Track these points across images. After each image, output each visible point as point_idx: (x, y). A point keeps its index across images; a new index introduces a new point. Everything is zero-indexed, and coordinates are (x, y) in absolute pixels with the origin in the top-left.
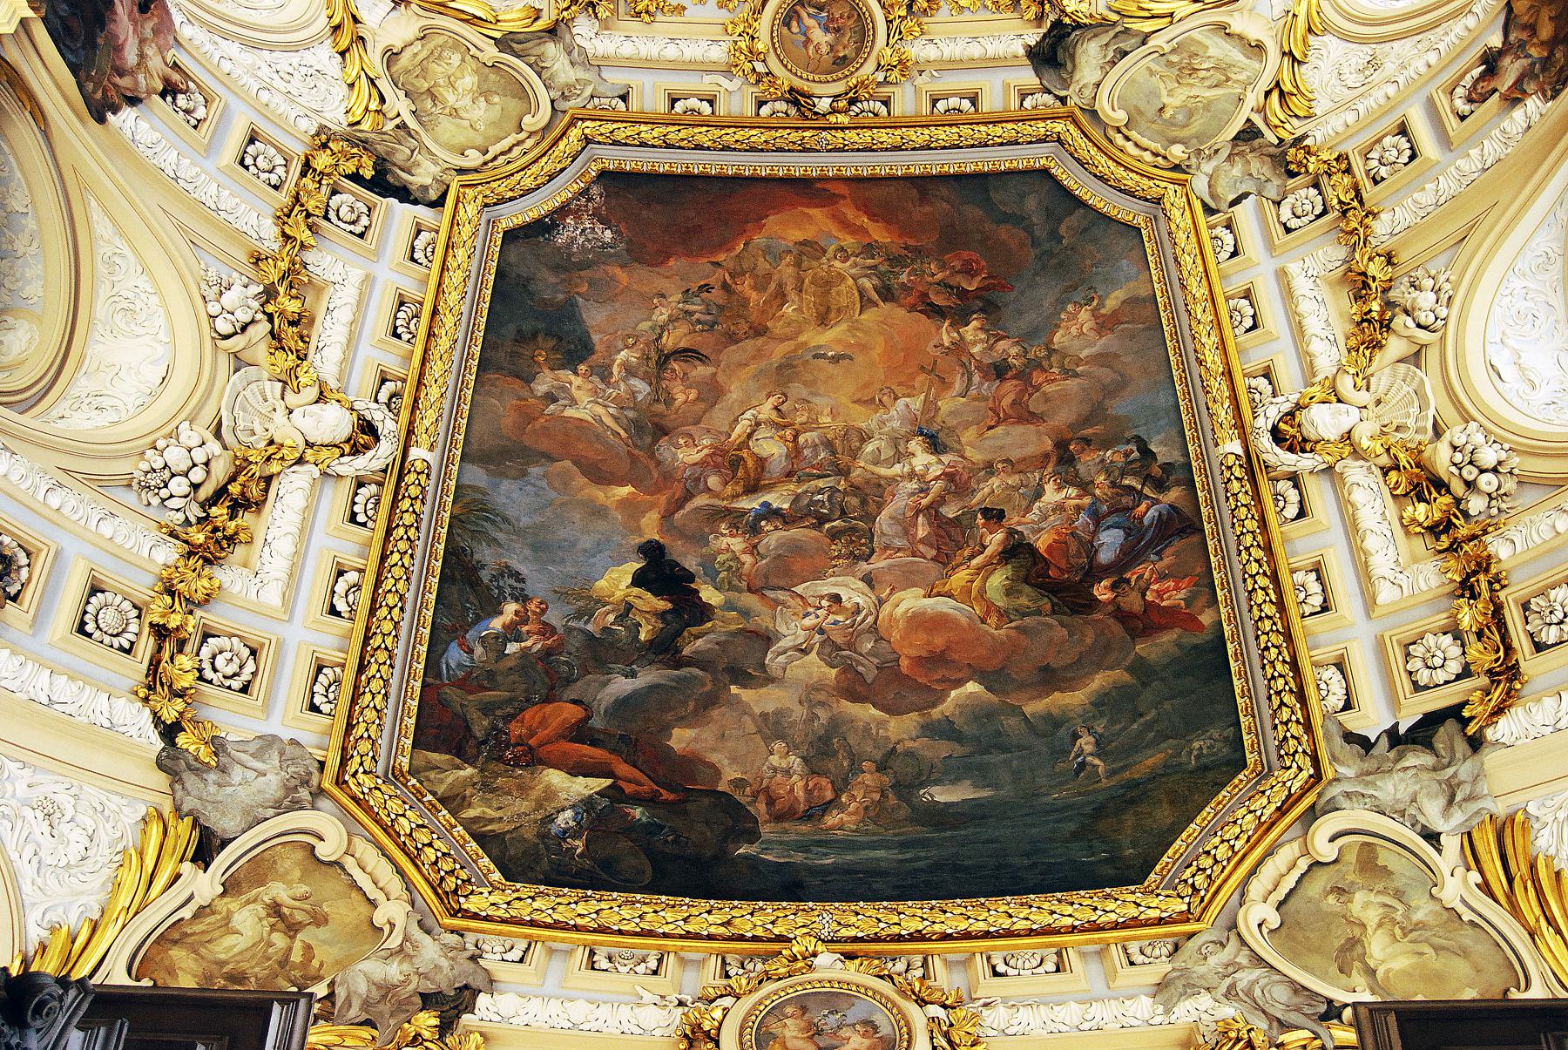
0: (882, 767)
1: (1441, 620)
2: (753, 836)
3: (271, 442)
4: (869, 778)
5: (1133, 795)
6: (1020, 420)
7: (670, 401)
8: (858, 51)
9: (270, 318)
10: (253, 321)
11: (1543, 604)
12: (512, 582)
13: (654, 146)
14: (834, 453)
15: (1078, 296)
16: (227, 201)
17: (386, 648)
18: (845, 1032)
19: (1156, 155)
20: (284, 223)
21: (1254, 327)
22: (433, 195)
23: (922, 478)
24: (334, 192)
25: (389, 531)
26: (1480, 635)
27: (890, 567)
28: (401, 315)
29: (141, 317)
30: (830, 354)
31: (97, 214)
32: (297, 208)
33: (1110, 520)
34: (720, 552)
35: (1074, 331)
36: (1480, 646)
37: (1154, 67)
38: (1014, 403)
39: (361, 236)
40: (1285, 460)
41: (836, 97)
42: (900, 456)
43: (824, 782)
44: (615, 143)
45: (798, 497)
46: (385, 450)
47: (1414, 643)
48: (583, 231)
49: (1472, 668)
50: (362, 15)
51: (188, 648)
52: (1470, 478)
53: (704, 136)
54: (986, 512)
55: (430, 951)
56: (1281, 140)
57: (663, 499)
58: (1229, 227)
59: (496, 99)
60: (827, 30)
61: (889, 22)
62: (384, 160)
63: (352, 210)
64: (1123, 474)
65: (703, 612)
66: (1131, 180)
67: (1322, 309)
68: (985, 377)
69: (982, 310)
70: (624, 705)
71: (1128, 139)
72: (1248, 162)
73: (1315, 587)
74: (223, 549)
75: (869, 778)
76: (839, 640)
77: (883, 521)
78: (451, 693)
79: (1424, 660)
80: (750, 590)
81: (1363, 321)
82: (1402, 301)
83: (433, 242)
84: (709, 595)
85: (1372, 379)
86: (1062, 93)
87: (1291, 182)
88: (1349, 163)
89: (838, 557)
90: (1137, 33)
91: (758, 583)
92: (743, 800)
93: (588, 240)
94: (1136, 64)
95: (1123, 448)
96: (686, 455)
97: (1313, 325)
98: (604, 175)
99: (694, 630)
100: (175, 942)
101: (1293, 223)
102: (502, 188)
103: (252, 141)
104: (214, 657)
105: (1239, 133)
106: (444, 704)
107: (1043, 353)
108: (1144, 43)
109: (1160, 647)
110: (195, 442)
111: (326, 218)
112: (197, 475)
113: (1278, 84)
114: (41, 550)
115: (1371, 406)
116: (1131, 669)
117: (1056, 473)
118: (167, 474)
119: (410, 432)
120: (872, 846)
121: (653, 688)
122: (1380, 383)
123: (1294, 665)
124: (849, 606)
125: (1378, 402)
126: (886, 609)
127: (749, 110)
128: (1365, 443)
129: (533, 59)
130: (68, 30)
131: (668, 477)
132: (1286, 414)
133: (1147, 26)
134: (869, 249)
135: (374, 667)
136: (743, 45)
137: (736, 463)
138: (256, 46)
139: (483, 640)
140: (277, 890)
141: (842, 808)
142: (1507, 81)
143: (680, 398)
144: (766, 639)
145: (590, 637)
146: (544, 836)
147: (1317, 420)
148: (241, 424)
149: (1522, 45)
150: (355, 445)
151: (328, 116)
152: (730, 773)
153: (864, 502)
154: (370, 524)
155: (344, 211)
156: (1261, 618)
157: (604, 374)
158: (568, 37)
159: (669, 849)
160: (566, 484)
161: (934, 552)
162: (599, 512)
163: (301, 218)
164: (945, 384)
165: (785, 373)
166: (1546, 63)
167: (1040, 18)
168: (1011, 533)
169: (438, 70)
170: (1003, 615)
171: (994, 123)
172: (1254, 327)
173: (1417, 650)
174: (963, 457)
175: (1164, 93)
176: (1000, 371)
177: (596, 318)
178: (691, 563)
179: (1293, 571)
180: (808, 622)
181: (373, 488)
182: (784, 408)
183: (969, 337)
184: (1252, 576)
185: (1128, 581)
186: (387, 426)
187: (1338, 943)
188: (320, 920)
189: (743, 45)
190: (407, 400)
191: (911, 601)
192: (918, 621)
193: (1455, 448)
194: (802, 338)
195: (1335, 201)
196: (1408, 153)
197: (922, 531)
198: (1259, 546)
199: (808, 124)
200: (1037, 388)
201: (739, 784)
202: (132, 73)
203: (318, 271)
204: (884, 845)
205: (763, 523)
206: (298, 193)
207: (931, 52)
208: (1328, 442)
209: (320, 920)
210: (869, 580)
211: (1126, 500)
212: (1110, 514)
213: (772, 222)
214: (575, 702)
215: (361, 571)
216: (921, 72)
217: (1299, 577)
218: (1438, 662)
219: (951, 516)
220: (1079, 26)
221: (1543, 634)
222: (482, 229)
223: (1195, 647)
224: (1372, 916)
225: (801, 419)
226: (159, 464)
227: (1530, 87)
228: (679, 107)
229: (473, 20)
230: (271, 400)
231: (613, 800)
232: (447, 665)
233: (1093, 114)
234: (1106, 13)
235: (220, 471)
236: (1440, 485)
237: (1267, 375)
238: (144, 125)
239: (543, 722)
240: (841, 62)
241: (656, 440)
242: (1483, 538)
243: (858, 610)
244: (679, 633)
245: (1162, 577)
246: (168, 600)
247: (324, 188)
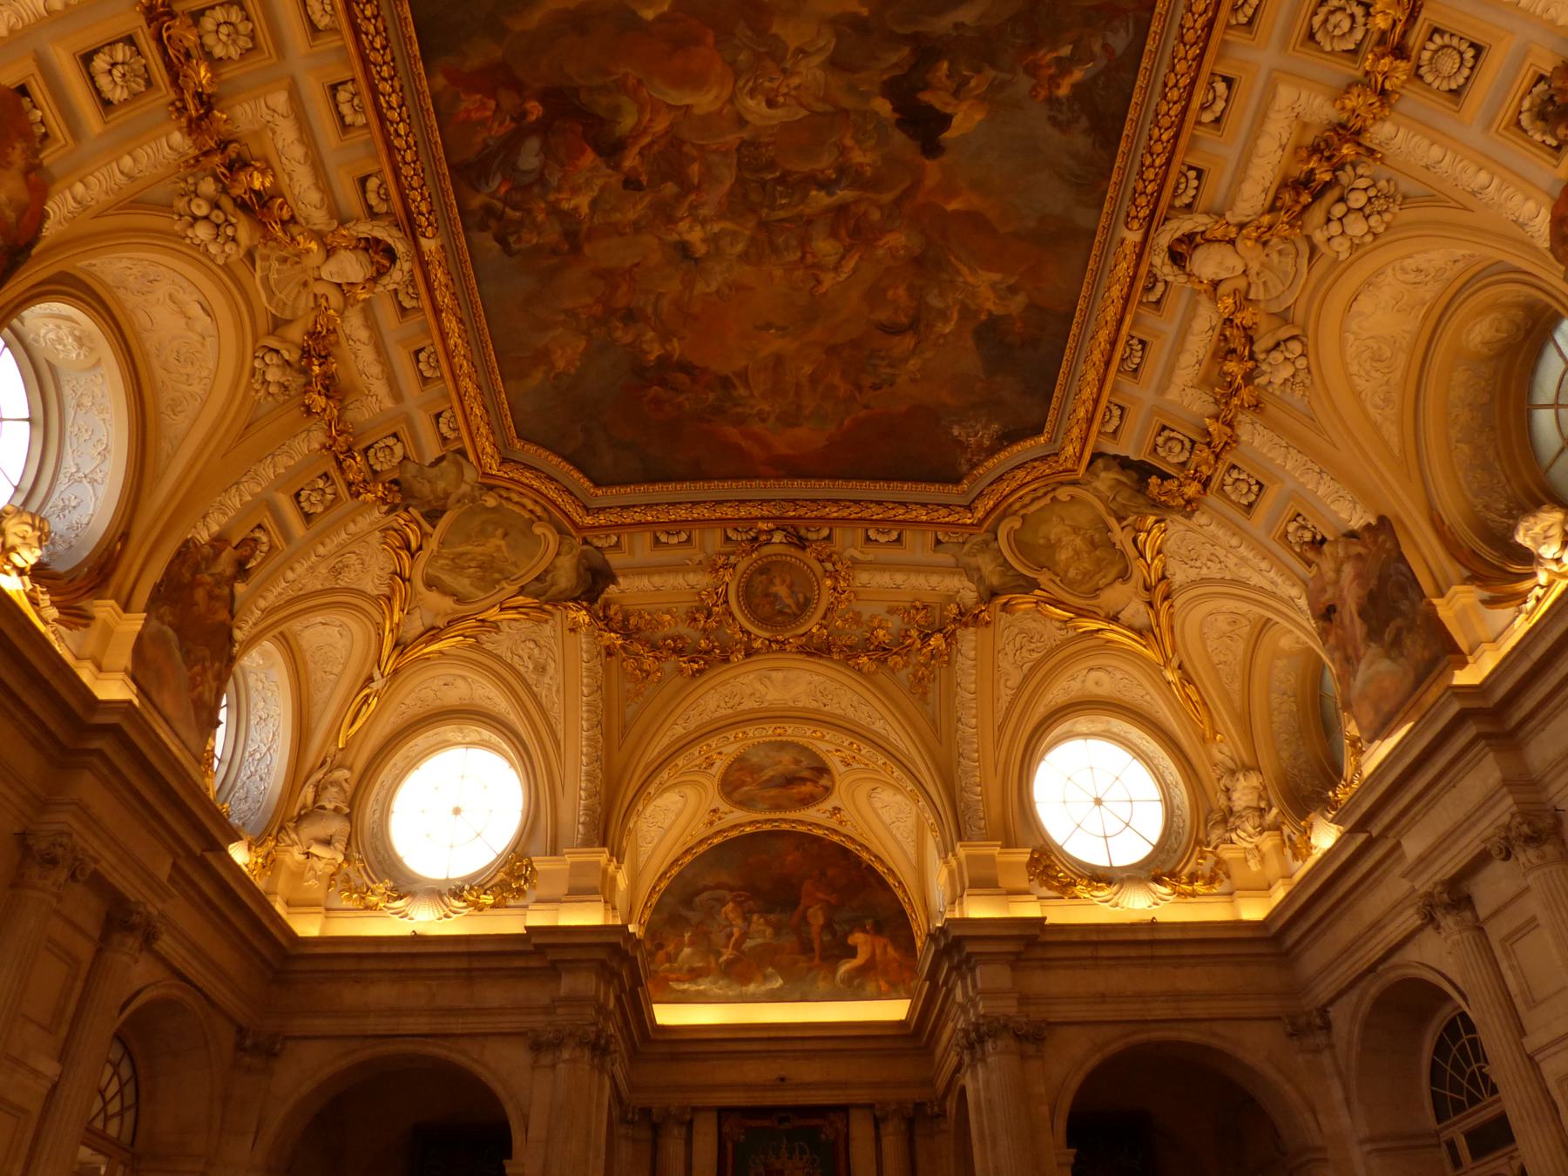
1: (228, 72)
3: (1265, 244)
8: (750, 580)
9: (1252, 356)
10: (1268, 352)
11: (134, 85)
12: (1061, 117)
13: (916, 504)
16: (1277, 456)
17: (1185, 45)
19: (508, 499)
20: (1231, 437)
21: (417, 353)
22: (1100, 463)
24: (1184, 464)
25: (1168, 162)
26: (188, 55)
28: (1137, 360)
29: (1367, 355)
30: (773, 331)
31: (1394, 441)
32: (1218, 450)
35: (569, 351)
36: (186, 44)
37: (513, 569)
39: (1164, 428)
40: (381, 232)
41: (768, 542)
42: (713, 240)
44: (947, 506)
45: (804, 199)
46: (1164, 238)
47: (248, 50)
48: (976, 435)
49: (190, 21)
50: (1143, 608)
51: (1375, 37)
52: (216, 212)
53: (876, 512)
54: (638, 187)
56: (406, 510)
58: (444, 439)
59: (1041, 541)
60: (776, 596)
61: (726, 602)
62: (1139, 491)
63: (1170, 450)
64: (521, 223)
66: (527, 477)
67: (361, 367)
71: (531, 512)
72: (433, 492)
73: (345, 109)
74: (1326, 141)
77: (728, 178)
79: (237, 32)
80: (846, 112)
81: (325, 357)
82: (294, 373)
83: (1104, 423)
84: (883, 107)
85: (312, 305)
86: (585, 547)
87: (396, 475)
88: (349, 490)
89: (768, 144)
90: (526, 596)
93: (972, 426)
94: (528, 571)
95: (523, 246)
96: (898, 240)
97: (367, 355)
98: (957, 481)
99: (898, 72)
101: (391, 441)
102: (1043, 468)
103: (1250, 505)
104: (1352, 29)
105: (441, 516)
107: (594, 331)
108: (522, 588)
109: (480, 54)
110: (1335, 242)
111: (1193, 442)
112: (1339, 210)
113: (412, 556)
114: (1506, 128)
115: (311, 280)
118: (1367, 211)
119: (1140, 256)
122: (306, 302)
123: (356, 31)
124: (760, 97)
125: (305, 284)
126: (726, 93)
127: (837, 532)
128: (314, 246)
129: (1011, 573)
130: (1403, 589)
132: (383, 274)
133: (521, 600)
135: (1198, 25)
136: (842, 584)
138: (1235, 582)
142: (227, 557)
143: (901, 291)
147: (358, 267)
148: (1290, 260)
149: (218, 584)
150: (1191, 242)
151: (1182, 528)
154: (1184, 169)
155: (1177, 448)
156: (392, 78)
157: (966, 312)
158: (982, 589)
161: (687, 148)
163: (1216, 441)
166: (196, 569)
167: (606, 606)
168: (616, 167)
169: (1087, 565)
171: (640, 523)
172: (417, 353)
173: (244, 42)
174: (660, 239)
175: (504, 548)
176: (630, 316)
178: (899, 137)
179: (366, 126)
180: (796, 81)
181: (1178, 203)
182: (813, 283)
184: (402, 120)
185: (513, 119)
186: (1159, 260)
189: (842, 584)
190: (1140, 285)
191: (705, 101)
192: (695, 81)
193: (234, 239)
195: (358, 459)
196: (302, 499)
197: (695, 170)
198: (399, 150)
199: (792, 522)
202: (1348, 558)
203: (1205, 397)
205: (834, 176)
206: (1216, 462)
207: (693, 579)
208: (346, 248)
210: (741, 122)
211: (517, 197)
212: (531, 185)
215: (1199, 123)
216: (700, 563)
217: (361, 120)
218: (224, 30)
219: (670, 184)
220: (575, 600)
221: (128, 53)
222: (1061, 436)
225: (799, 273)
226: (1374, 220)
227: (207, 550)
228: (894, 535)
229: (1056, 603)
230: (1260, 282)
232: (1128, 31)
233: (561, 531)
234: (554, 611)
235: (1317, 214)
236: (242, 206)
237: (403, 311)
238: (1344, 515)
240: (764, 570)
242: (197, 152)
246: (1388, 85)
247: (1193, 466)
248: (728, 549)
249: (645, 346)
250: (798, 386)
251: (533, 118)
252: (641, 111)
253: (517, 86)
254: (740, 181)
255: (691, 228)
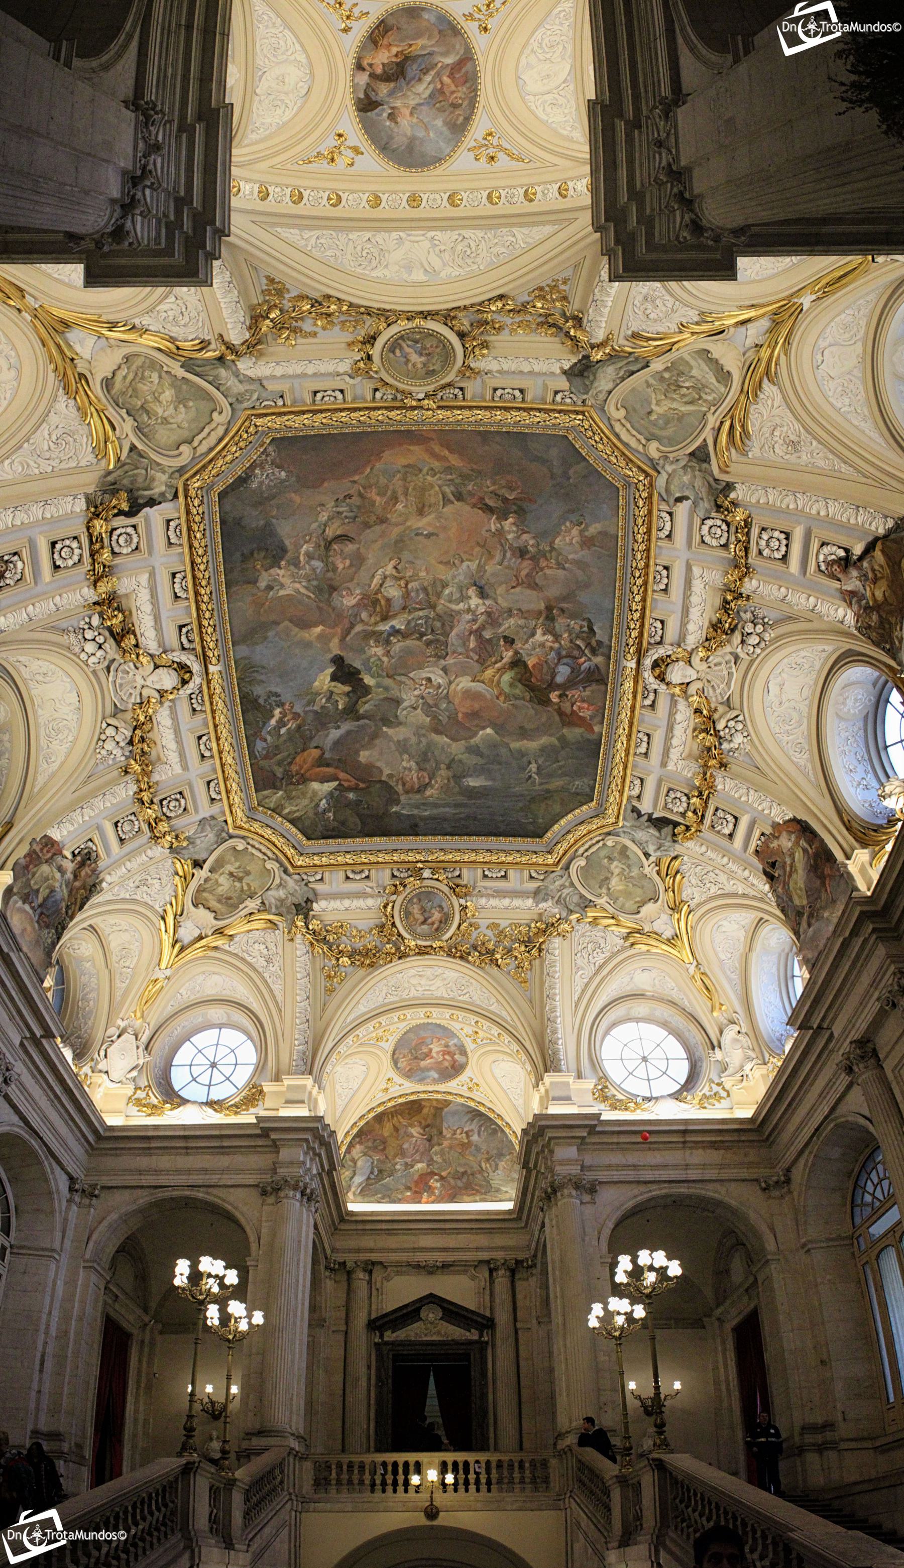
0: (449, 767)
2: (397, 802)
4: (443, 772)
5: (547, 795)
6: (529, 587)
7: (335, 569)
14: (427, 594)
15: (574, 517)
18: (433, 911)
23: (474, 612)
27: (455, 664)
33: (565, 660)
34: (371, 657)
35: (567, 539)
38: (527, 575)
42: (464, 598)
43: (425, 774)
45: (409, 622)
54: (505, 637)
55: (290, 882)
57: (339, 630)
64: (577, 637)
65: (367, 690)
68: (513, 555)
69: (515, 512)
70: (337, 743)
75: (443, 772)
76: (431, 702)
78: (263, 763)
80: (388, 676)
84: (368, 680)
91: (391, 673)
92: (393, 784)
95: (580, 622)
99: (364, 700)
100: (204, 891)
106: (262, 769)
107: (548, 548)
109: (573, 733)
116: (558, 739)
117: (543, 624)
120: (444, 806)
121: (349, 733)
126: (453, 686)
131: (340, 616)
134: (449, 469)
137: (376, 602)
139: (269, 733)
140: (229, 868)
141: (432, 787)
143: (341, 566)
144: (398, 702)
145: (316, 713)
146: (316, 814)
152: (386, 771)
153: (443, 625)
157: (296, 563)
159: (366, 812)
160: (288, 635)
162: (308, 645)
164: (491, 556)
165: (399, 545)
168: (517, 653)
170: (507, 697)
176: (522, 553)
177: (285, 530)
178: (357, 664)
180: (417, 693)
182: (399, 567)
183: (507, 528)
187: (602, 877)
188: (248, 873)
191: (464, 683)
194: (408, 524)
197: (472, 644)
200: (542, 569)
201: (390, 776)
204: (447, 805)
209: (248, 873)
210: (445, 670)
211: (576, 653)
212: (566, 657)
213: (387, 455)
214: (316, 747)
223: (588, 740)
224: (617, 871)
225: (409, 574)
231: (341, 791)
239: (305, 761)
241: (330, 594)
243: (439, 686)
244: (357, 702)
245: (583, 701)
248: (461, 385)
249: (515, 529)
250: (406, 494)
251: (557, 693)
252: (499, 682)
253: (561, 713)
254: (447, 635)
255: (477, 606)
